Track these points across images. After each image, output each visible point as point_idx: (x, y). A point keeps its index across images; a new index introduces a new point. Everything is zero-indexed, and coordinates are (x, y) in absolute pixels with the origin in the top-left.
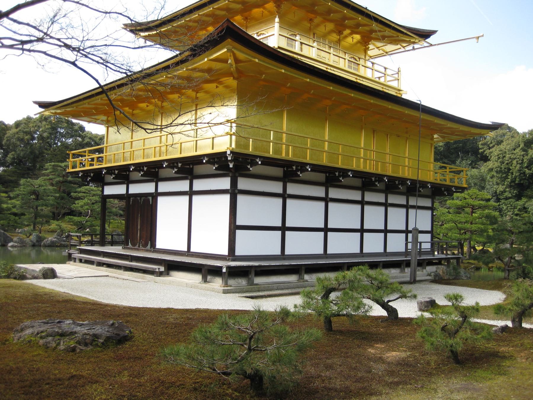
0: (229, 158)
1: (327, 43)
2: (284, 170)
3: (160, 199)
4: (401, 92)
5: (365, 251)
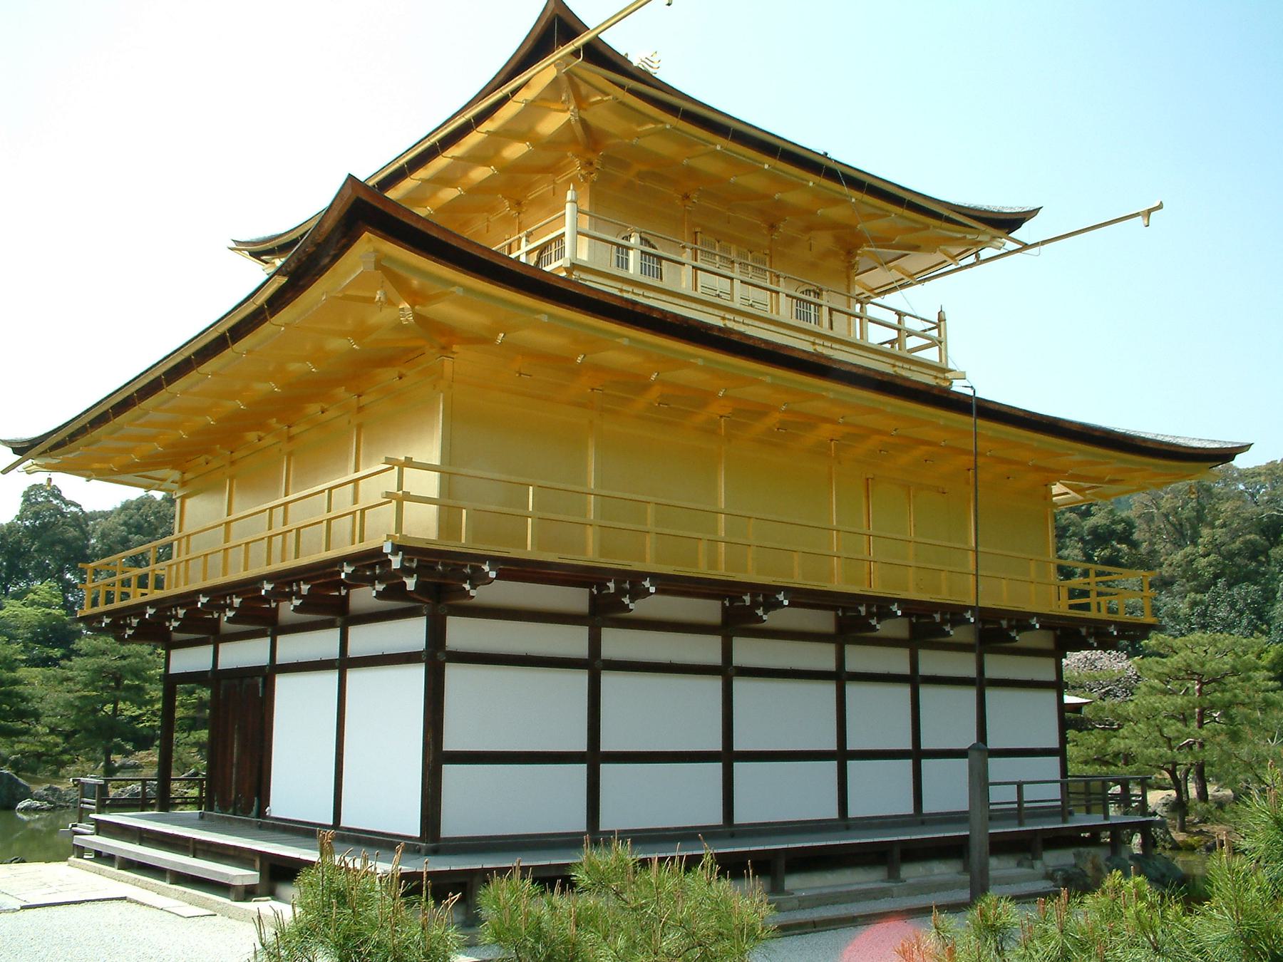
0: (396, 562)
1: (717, 251)
2: (591, 593)
3: (283, 683)
4: (949, 375)
5: (852, 813)
